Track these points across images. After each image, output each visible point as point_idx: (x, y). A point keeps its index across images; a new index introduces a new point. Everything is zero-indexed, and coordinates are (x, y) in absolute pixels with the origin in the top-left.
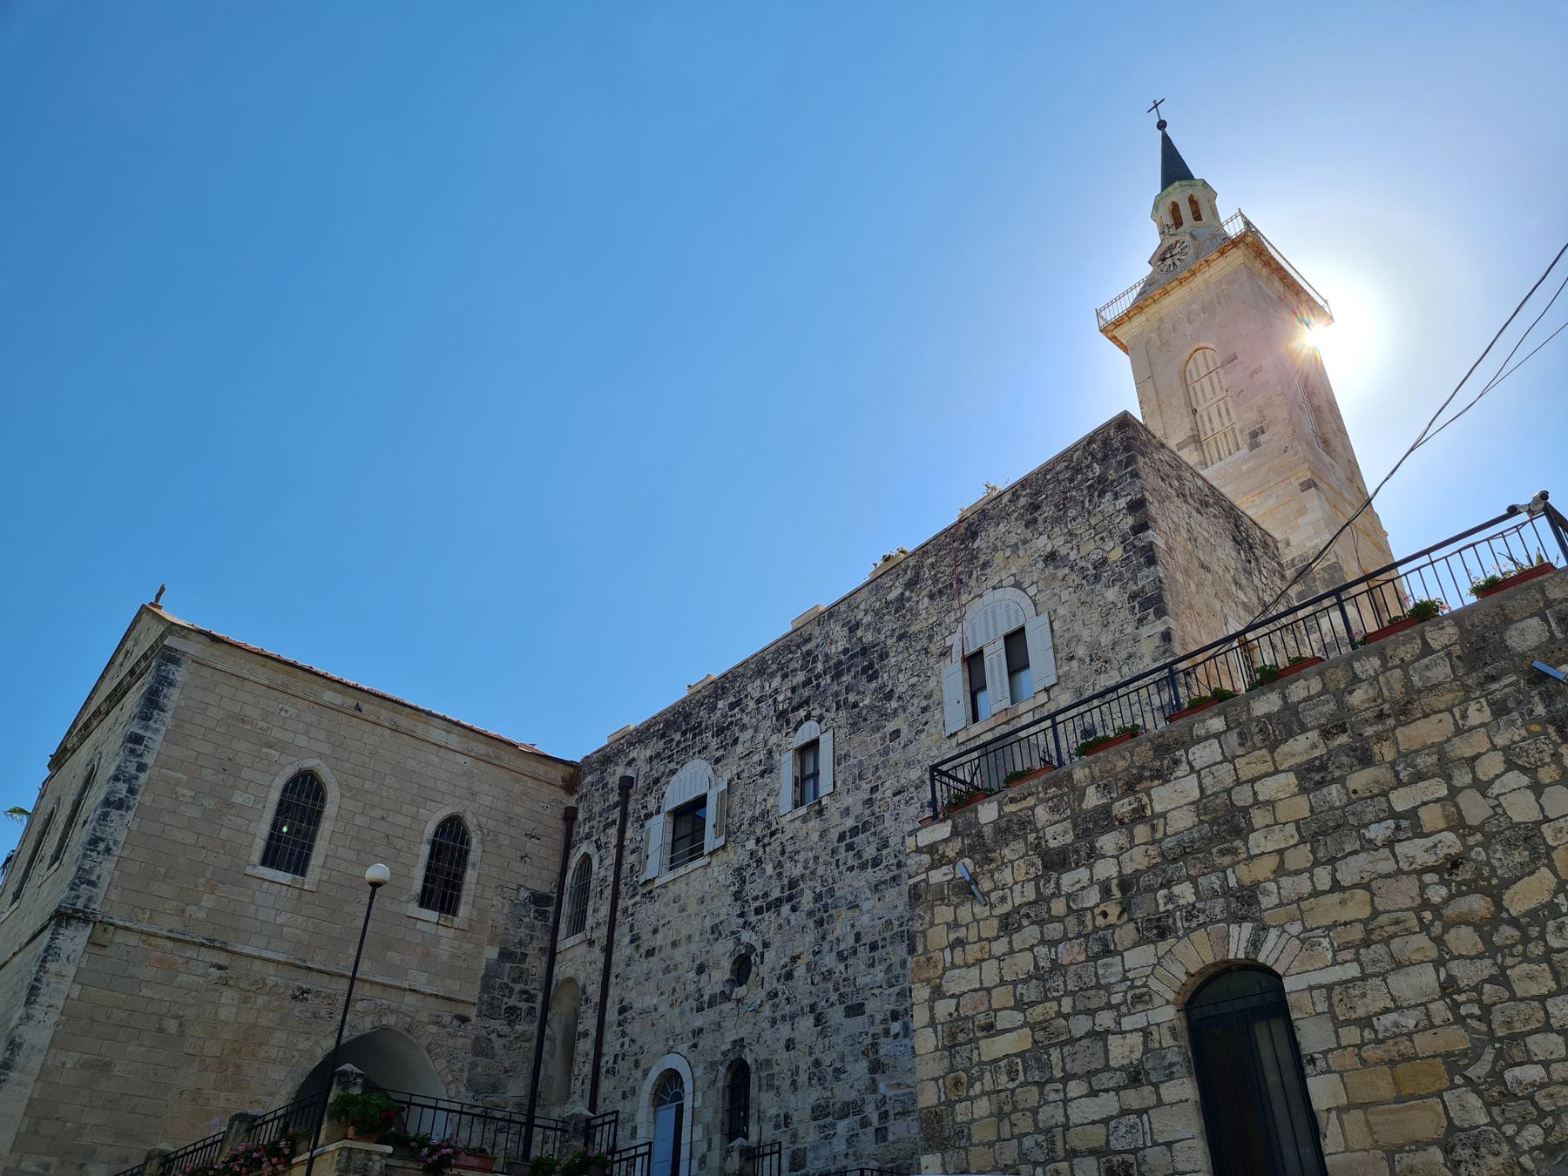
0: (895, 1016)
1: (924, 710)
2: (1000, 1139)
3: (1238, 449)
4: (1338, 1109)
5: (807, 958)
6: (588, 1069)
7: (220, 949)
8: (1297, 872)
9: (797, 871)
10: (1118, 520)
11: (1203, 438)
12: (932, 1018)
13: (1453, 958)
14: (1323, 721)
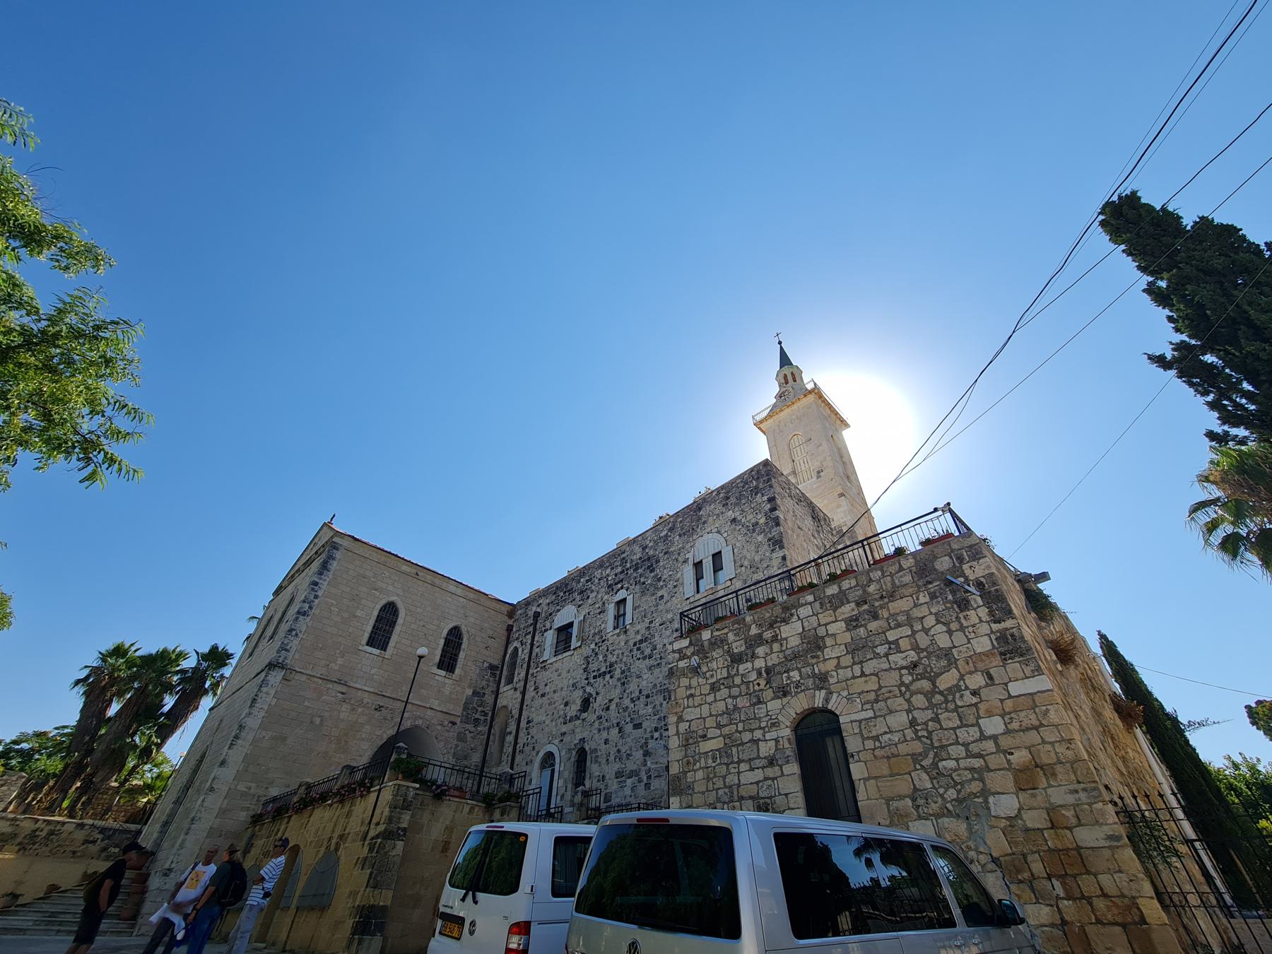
0: (656, 729)
1: (675, 587)
2: (707, 791)
4: (864, 779)
5: (617, 700)
6: (510, 749)
8: (846, 667)
9: (614, 660)
12: (678, 731)
13: (915, 709)
14: (857, 598)
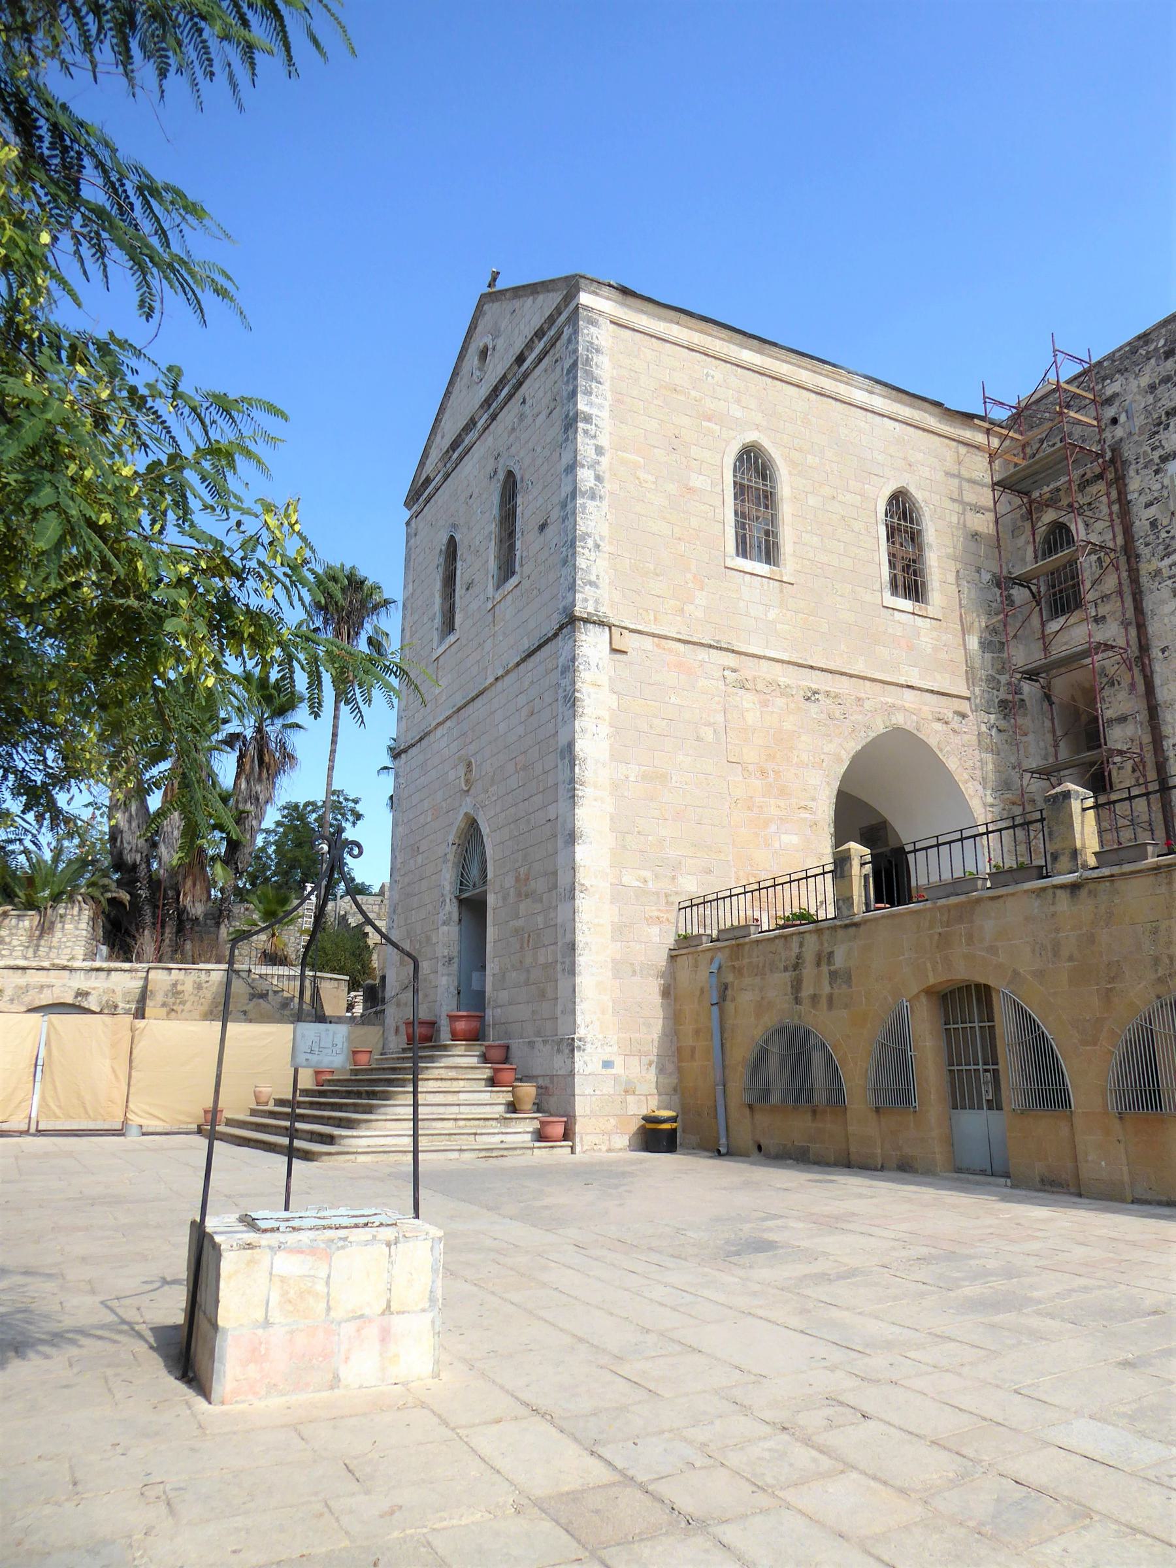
7: (727, 650)
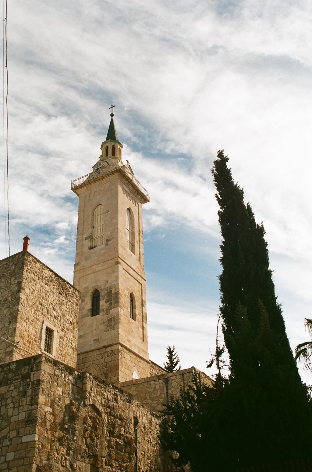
3: (103, 244)
10: (14, 287)
11: (94, 237)
